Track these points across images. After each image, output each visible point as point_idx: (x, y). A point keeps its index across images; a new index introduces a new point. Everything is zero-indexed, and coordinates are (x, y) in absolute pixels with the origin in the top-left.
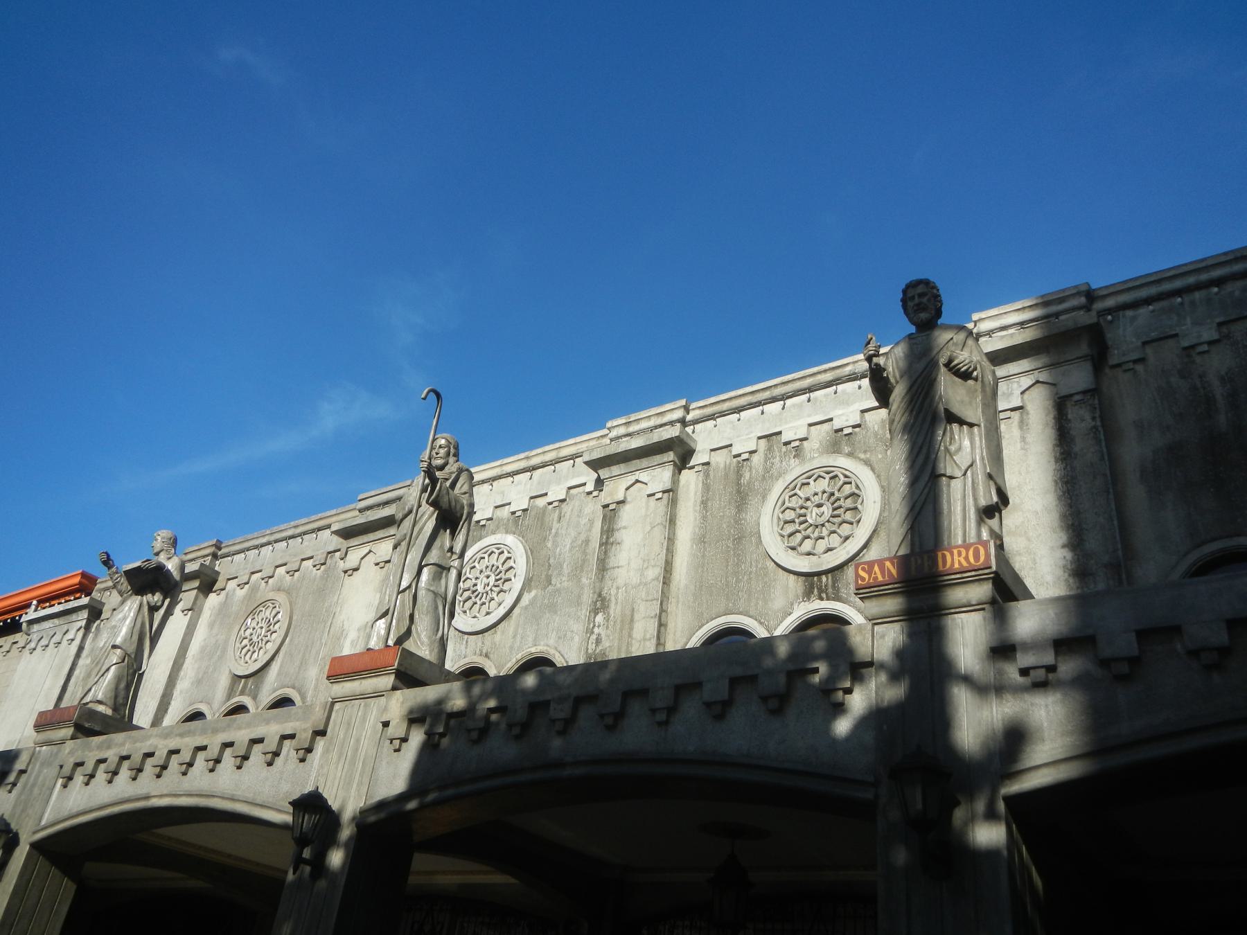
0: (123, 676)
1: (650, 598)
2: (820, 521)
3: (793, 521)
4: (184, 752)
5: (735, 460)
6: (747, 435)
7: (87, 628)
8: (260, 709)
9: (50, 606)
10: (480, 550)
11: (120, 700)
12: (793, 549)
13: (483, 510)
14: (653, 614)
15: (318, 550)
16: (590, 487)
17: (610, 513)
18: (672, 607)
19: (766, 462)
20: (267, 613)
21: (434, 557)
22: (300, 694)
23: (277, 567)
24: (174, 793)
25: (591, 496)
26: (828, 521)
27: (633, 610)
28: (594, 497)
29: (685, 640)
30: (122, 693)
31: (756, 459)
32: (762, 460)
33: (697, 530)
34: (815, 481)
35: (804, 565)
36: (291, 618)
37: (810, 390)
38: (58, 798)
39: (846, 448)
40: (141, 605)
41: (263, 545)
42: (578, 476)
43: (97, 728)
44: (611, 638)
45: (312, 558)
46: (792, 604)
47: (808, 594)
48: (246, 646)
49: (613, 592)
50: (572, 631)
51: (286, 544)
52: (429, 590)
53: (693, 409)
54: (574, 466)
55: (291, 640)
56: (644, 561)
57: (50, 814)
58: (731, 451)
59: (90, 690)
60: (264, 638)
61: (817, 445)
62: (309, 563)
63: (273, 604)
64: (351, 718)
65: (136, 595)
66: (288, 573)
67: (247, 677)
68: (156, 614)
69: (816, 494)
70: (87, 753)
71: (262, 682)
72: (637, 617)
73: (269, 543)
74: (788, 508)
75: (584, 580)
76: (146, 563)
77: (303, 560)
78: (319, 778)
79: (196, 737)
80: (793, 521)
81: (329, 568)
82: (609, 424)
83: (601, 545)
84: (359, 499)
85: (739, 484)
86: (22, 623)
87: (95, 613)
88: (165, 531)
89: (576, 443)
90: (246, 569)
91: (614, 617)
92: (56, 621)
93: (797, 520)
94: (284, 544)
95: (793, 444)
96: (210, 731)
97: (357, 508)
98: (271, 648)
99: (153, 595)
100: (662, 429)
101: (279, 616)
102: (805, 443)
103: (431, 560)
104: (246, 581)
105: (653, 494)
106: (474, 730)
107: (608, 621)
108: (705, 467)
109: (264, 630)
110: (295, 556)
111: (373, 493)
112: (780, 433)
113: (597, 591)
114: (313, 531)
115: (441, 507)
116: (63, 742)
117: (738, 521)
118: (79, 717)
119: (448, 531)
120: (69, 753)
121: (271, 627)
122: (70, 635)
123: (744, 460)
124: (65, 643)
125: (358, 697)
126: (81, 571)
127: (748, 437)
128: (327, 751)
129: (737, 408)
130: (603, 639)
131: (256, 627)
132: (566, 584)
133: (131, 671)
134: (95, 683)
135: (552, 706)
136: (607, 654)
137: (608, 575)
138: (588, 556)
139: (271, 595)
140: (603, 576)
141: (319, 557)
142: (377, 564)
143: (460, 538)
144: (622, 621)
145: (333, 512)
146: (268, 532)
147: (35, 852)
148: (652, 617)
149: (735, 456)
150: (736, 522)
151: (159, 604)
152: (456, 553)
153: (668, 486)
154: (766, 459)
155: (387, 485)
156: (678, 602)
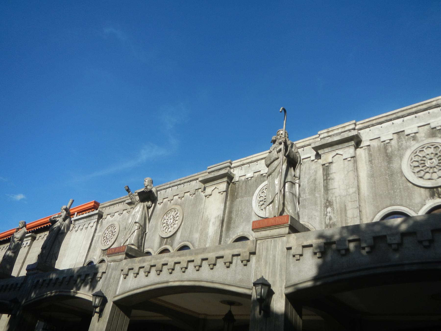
0: (140, 235)
1: (353, 200)
2: (433, 165)
3: (418, 166)
4: (183, 263)
5: (382, 143)
6: (387, 133)
7: (98, 222)
8: (175, 250)
9: (82, 214)
10: (265, 185)
11: (140, 244)
12: (421, 177)
13: (264, 170)
14: (356, 207)
15: (191, 189)
16: (313, 158)
17: (326, 168)
18: (362, 204)
19: (398, 143)
20: (173, 213)
21: (289, 178)
22: (191, 244)
23: (174, 196)
24: (181, 280)
25: (314, 162)
26: (437, 165)
27: (345, 206)
28: (315, 162)
29: (372, 217)
30: (140, 241)
31: (393, 142)
32: (396, 143)
33: (369, 173)
34: (426, 149)
35: (429, 184)
36: (183, 215)
37: (416, 112)
38: (122, 283)
39: (439, 135)
40: (144, 206)
41: (167, 188)
42: (306, 154)
43: (133, 255)
44: (337, 217)
45: (189, 192)
46: (425, 201)
47: (432, 196)
48: (165, 226)
49: (334, 199)
50: (315, 216)
51: (177, 187)
52: (290, 192)
53: (358, 124)
54: (303, 150)
55: (184, 224)
56: (347, 186)
57: (120, 289)
58: (380, 140)
59: (127, 240)
60: (172, 223)
61: (423, 135)
62: (188, 194)
63: (174, 210)
64: (267, 246)
65: (141, 202)
66: (179, 198)
67: (167, 238)
68: (149, 210)
69: (428, 154)
70: (133, 264)
71: (174, 240)
72: (348, 208)
73: (170, 187)
74: (414, 161)
75: (317, 195)
76: (146, 189)
77: (185, 193)
78: (257, 273)
79: (187, 257)
80: (418, 166)
81: (197, 195)
82: (319, 133)
83: (324, 180)
84: (208, 168)
85: (386, 153)
86: (72, 221)
87: (100, 216)
88: (148, 178)
89: (303, 141)
90: (161, 197)
91: (336, 209)
92: (85, 220)
93: (420, 166)
94: (176, 187)
95: (411, 135)
96: (194, 254)
97: (208, 172)
98: (176, 226)
99: (148, 202)
100: (344, 133)
101: (178, 214)
102: (417, 134)
103: (289, 180)
104: (162, 202)
105: (346, 159)
106: (342, 249)
107: (333, 210)
108: (368, 147)
109: (172, 220)
110: (181, 191)
112: (404, 131)
113: (326, 198)
114: (188, 182)
115: (290, 158)
116: (121, 260)
117: (389, 168)
118: (127, 250)
119: (292, 168)
120: (125, 265)
121: (175, 218)
122: (91, 225)
123: (387, 143)
124: (89, 227)
125: (270, 237)
126: (94, 201)
127: (387, 134)
128: (258, 261)
129: (380, 122)
130: (333, 218)
131: (169, 219)
132: (308, 197)
133: (143, 232)
134: (129, 237)
135: (388, 238)
136: (336, 224)
137: (330, 192)
138: (317, 186)
139: (173, 207)
140: (327, 193)
141: (192, 191)
142: (219, 193)
143: (298, 171)
144: (341, 210)
145: (196, 174)
146: (169, 183)
147: (115, 305)
148: (355, 208)
149: (382, 142)
150: (389, 168)
151: (150, 206)
152: (297, 177)
153: (353, 155)
154: (398, 142)
155: (218, 163)
156: (365, 202)
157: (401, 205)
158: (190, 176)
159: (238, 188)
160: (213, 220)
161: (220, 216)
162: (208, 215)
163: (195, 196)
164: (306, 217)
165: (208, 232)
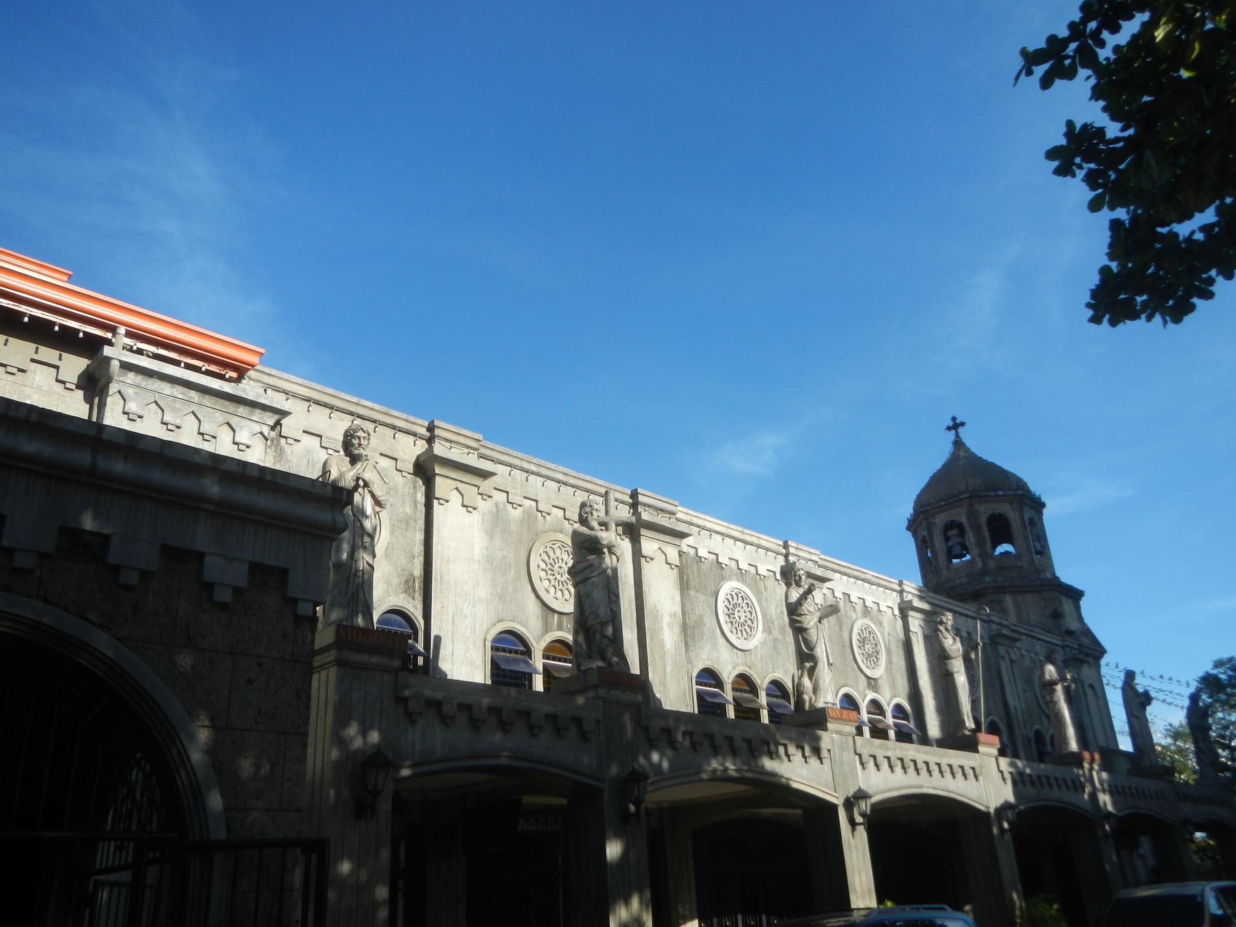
73: (538, 475)
92: (193, 394)
112: (849, 595)
158: (589, 478)
160: (666, 620)
164: (782, 668)
165: (663, 640)
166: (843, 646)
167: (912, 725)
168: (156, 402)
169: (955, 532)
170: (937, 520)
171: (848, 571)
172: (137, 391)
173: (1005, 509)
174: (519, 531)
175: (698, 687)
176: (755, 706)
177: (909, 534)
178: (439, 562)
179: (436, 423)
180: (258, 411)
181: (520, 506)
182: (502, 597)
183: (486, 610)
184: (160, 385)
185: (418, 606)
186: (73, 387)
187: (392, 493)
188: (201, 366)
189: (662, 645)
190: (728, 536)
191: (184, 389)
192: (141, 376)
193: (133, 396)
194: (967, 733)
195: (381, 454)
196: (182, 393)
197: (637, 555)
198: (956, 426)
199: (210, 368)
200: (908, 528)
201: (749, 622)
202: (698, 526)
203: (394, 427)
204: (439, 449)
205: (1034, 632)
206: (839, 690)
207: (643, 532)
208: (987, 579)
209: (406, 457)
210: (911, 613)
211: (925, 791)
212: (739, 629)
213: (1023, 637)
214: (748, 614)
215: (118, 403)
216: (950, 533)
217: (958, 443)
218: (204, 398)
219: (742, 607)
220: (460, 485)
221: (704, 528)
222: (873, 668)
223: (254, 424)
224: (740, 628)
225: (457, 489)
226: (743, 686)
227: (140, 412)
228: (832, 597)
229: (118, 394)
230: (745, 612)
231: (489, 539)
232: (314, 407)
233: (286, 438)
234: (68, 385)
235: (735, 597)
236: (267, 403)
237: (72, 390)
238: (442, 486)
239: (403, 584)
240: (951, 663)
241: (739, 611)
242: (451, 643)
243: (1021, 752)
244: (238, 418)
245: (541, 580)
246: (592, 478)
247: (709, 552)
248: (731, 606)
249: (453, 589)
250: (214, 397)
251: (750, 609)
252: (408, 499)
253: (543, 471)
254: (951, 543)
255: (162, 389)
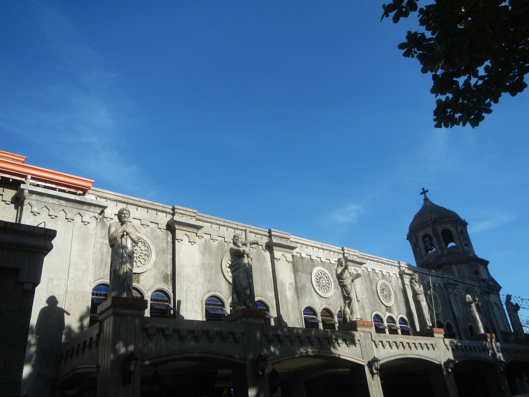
27: (363, 305)
72: (365, 307)
90: (215, 233)
92: (63, 202)
111: (284, 233)
112: (374, 270)
144: (362, 307)
157: (379, 311)
159: (297, 262)
160: (287, 286)
161: (293, 284)
162: (282, 279)
163: (256, 251)
165: (286, 295)
166: (373, 293)
167: (409, 327)
168: (46, 207)
169: (428, 239)
170: (419, 234)
171: (373, 259)
172: (37, 202)
173: (449, 227)
174: (217, 251)
175: (304, 315)
176: (333, 323)
177: (408, 241)
178: (179, 267)
179: (176, 207)
180: (92, 207)
181: (217, 240)
182: (209, 281)
183: (202, 287)
184: (47, 199)
185: (170, 288)
186: (9, 203)
187: (156, 238)
188: (66, 190)
189: (286, 297)
190: (315, 247)
191: (59, 200)
192: (39, 196)
193: (35, 205)
194: (428, 328)
195: (151, 222)
196: (57, 202)
197: (273, 258)
198: (424, 192)
199: (70, 190)
200: (407, 239)
201: (328, 285)
202: (301, 244)
203: (156, 210)
204: (177, 218)
205: (465, 281)
206: (373, 313)
207: (274, 248)
208: (444, 259)
209: (163, 222)
210: (405, 276)
211: (408, 356)
212: (323, 288)
213: (458, 283)
214: (327, 282)
215: (29, 208)
216: (426, 240)
217: (426, 200)
218: (68, 203)
219: (324, 278)
220: (187, 233)
221: (303, 244)
222: (389, 302)
223: (91, 213)
224: (323, 288)
225: (186, 235)
226: (327, 313)
227: (39, 211)
228: (367, 271)
229: (28, 204)
230: (325, 280)
231: (203, 256)
232: (140, 209)
233: (106, 218)
234: (7, 202)
235: (320, 274)
236: (96, 203)
237: (9, 204)
238: (179, 234)
239: (163, 278)
240: (418, 296)
241: (322, 280)
242: (185, 303)
243: (463, 337)
244: (84, 211)
245: (228, 272)
246: (250, 226)
247: (307, 255)
248: (319, 278)
249: (186, 279)
250: (72, 203)
251: (327, 279)
252: (164, 241)
253: (227, 224)
254: (426, 244)
255: (49, 201)
